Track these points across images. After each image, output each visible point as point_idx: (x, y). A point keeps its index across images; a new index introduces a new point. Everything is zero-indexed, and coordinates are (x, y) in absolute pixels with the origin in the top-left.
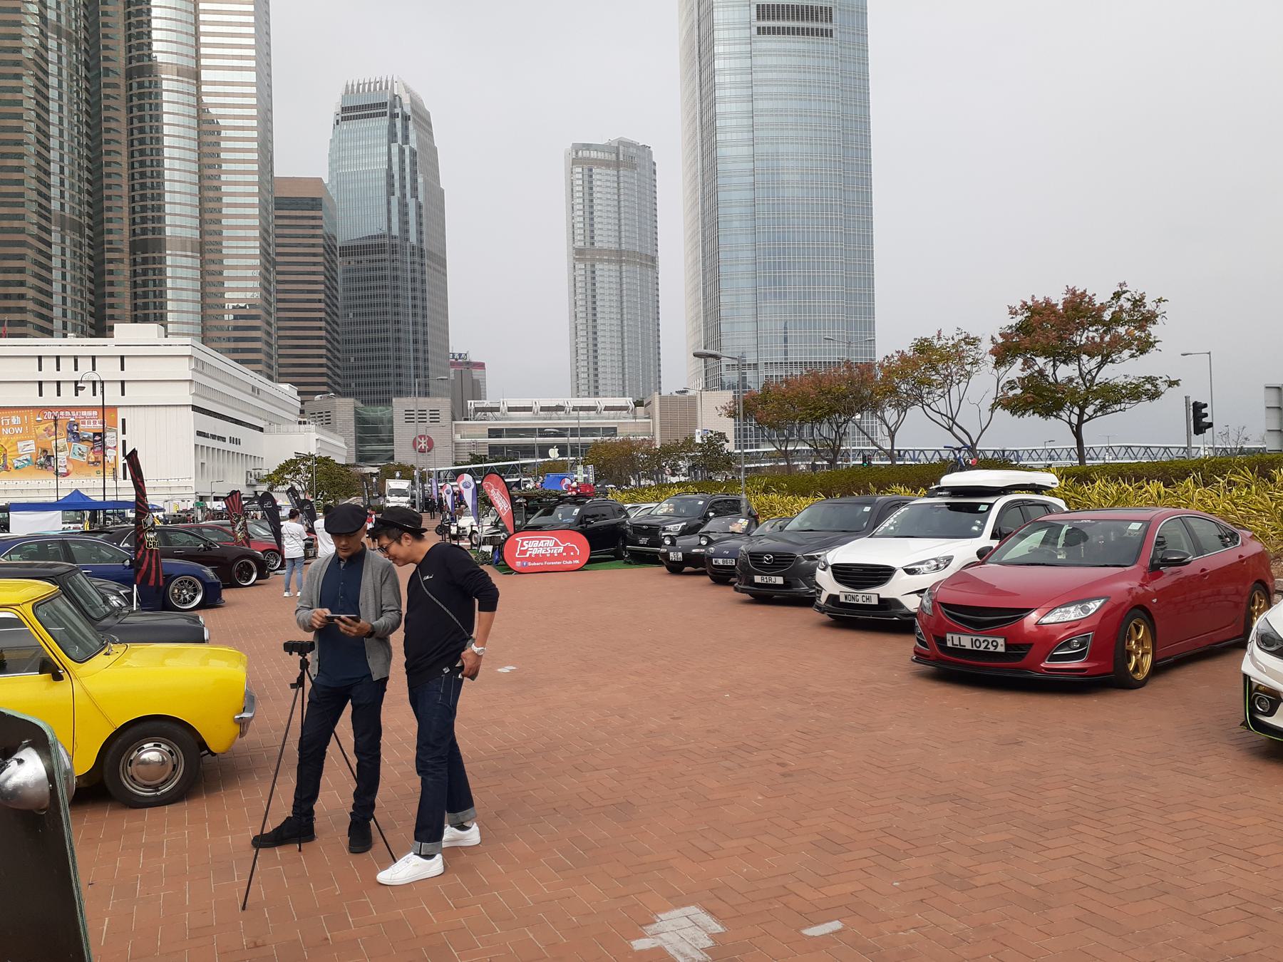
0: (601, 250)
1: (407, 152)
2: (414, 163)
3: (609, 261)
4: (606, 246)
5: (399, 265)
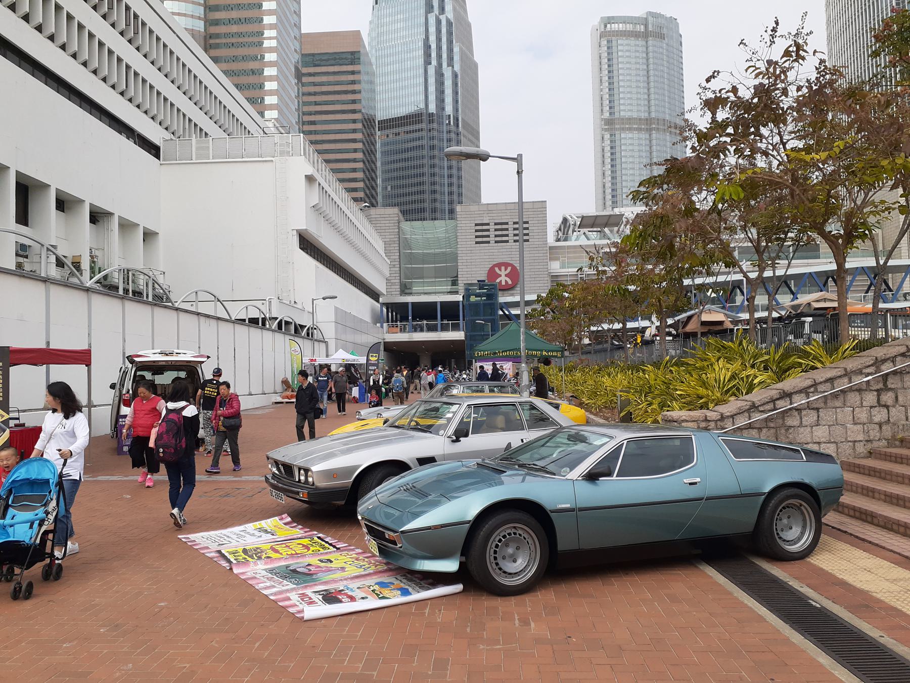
0: (630, 120)
1: (444, 23)
2: (450, 33)
3: (639, 130)
4: (635, 115)
5: (435, 133)
